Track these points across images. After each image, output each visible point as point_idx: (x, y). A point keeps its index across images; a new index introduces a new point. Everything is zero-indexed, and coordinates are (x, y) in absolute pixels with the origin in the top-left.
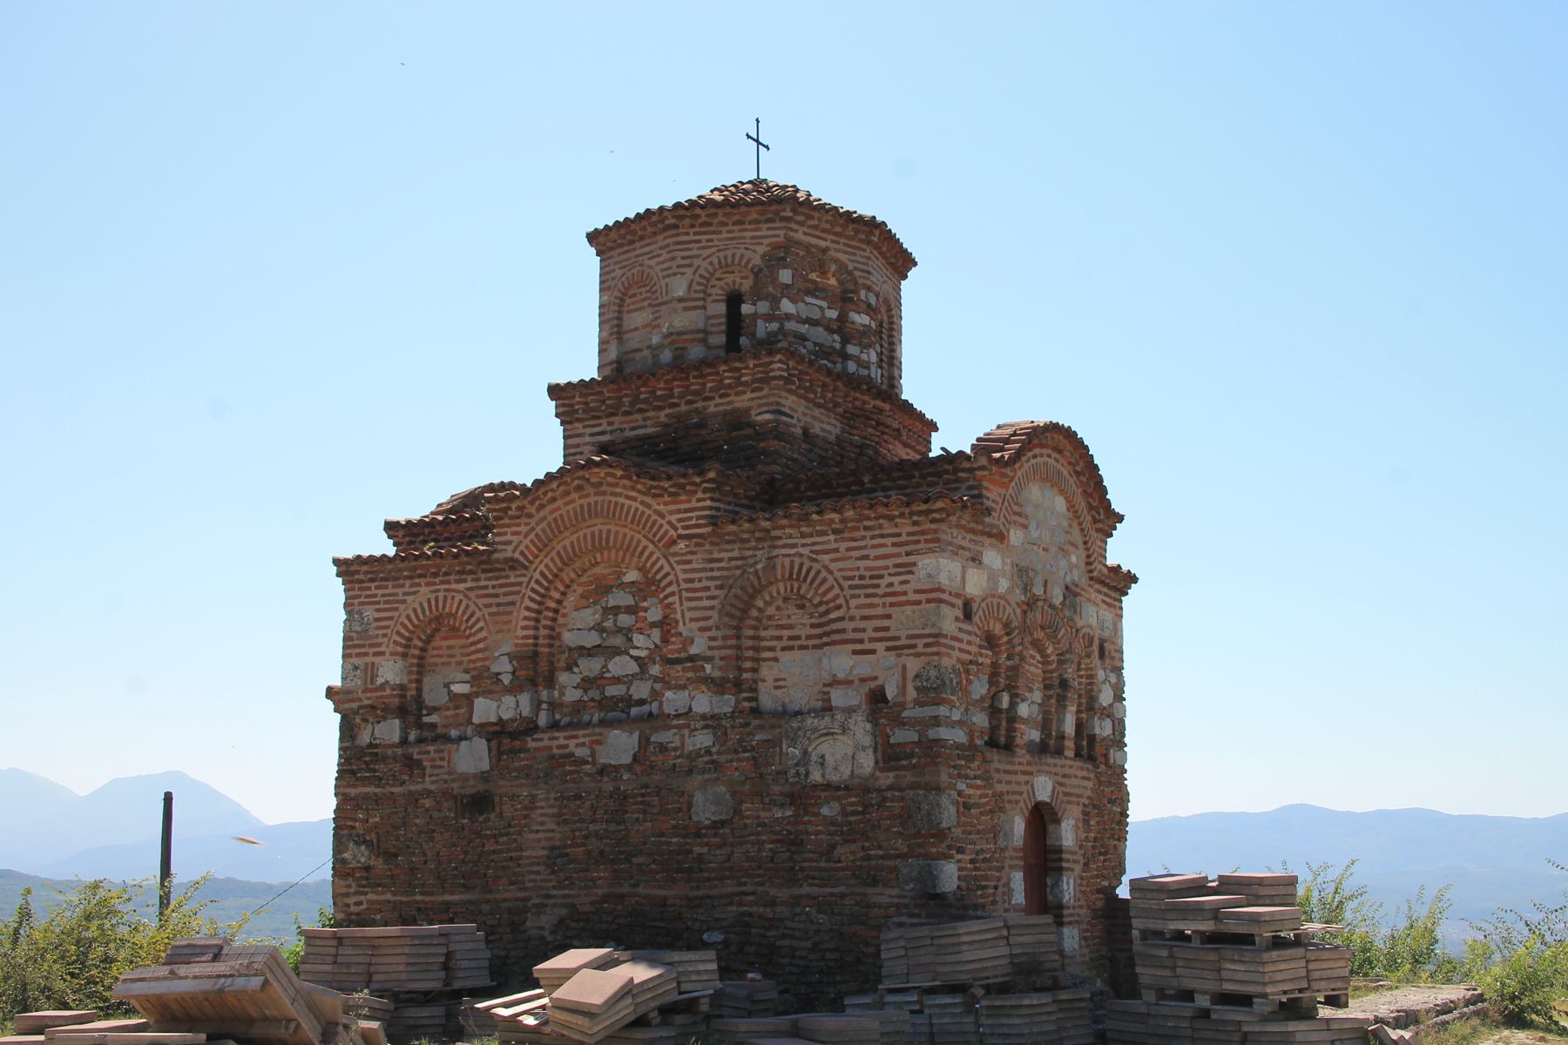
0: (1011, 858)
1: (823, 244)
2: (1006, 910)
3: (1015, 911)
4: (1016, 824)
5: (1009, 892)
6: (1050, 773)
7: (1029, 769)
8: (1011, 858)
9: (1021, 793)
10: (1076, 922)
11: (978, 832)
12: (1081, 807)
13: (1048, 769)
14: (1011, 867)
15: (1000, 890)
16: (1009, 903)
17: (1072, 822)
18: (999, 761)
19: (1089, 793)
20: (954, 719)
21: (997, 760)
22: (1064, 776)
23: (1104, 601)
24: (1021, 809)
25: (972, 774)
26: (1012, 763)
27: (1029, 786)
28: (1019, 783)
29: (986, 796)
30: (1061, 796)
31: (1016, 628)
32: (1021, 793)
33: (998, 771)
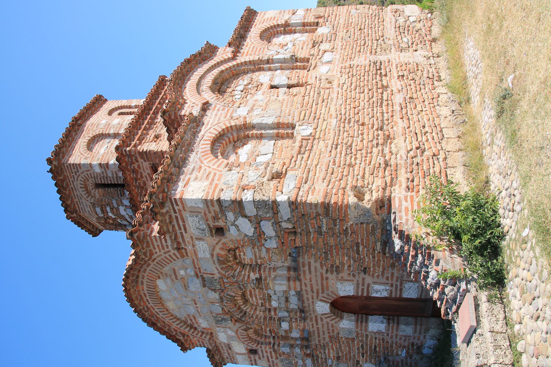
0: (361, 330)
1: (97, 224)
2: (388, 335)
3: (388, 330)
4: (344, 326)
5: (379, 332)
6: (313, 302)
7: (314, 319)
8: (361, 330)
9: (328, 323)
10: (401, 285)
11: (350, 352)
12: (329, 275)
13: (311, 304)
14: (366, 331)
15: (377, 336)
16: (384, 333)
17: (339, 285)
18: (315, 341)
19: (318, 265)
20: (302, 363)
21: (315, 341)
22: (313, 292)
23: (186, 232)
24: (336, 323)
25: (323, 356)
26: (314, 331)
27: (323, 317)
28: (323, 325)
29: (332, 348)
30: (325, 295)
31: (246, 327)
32: (328, 323)
33: (319, 341)
